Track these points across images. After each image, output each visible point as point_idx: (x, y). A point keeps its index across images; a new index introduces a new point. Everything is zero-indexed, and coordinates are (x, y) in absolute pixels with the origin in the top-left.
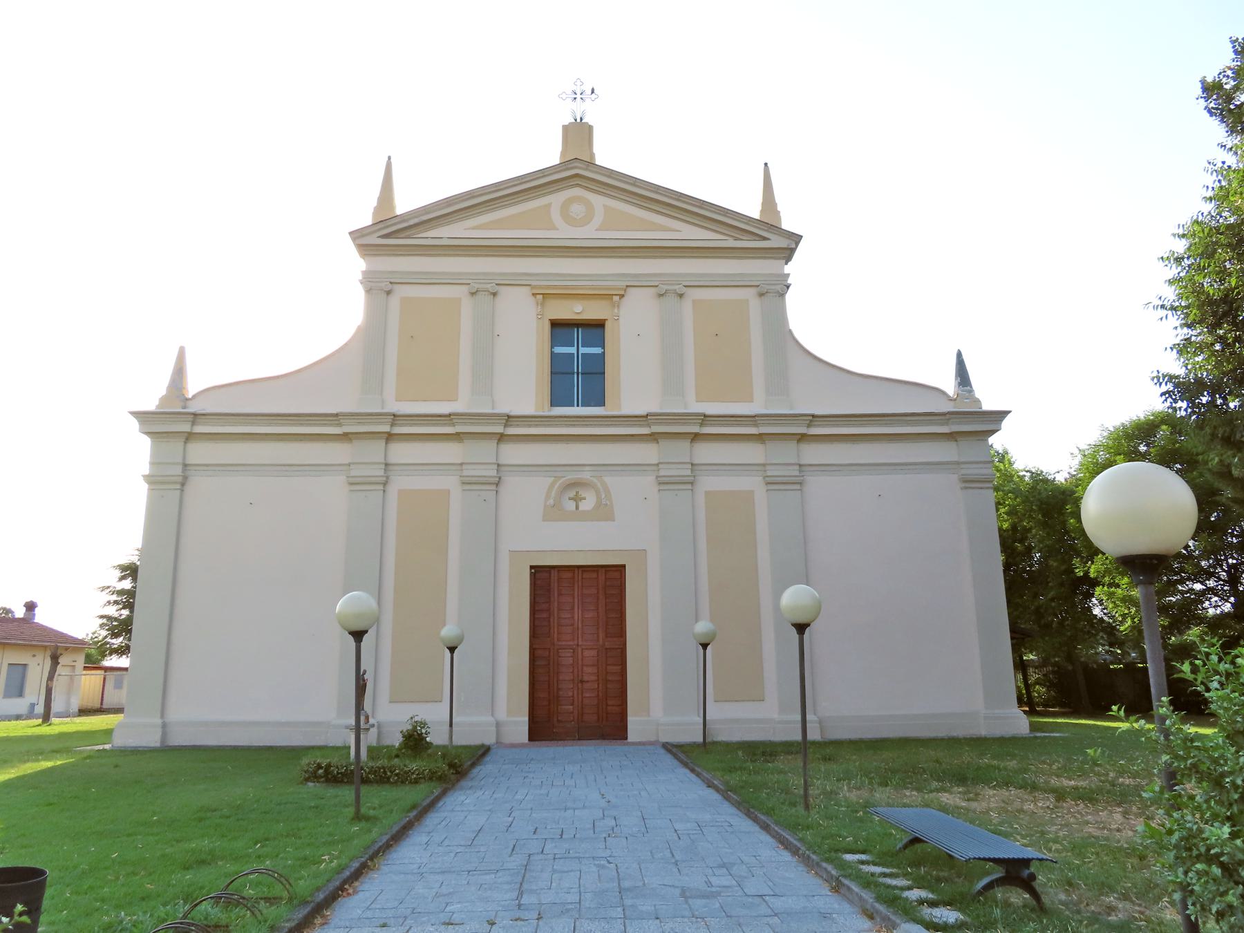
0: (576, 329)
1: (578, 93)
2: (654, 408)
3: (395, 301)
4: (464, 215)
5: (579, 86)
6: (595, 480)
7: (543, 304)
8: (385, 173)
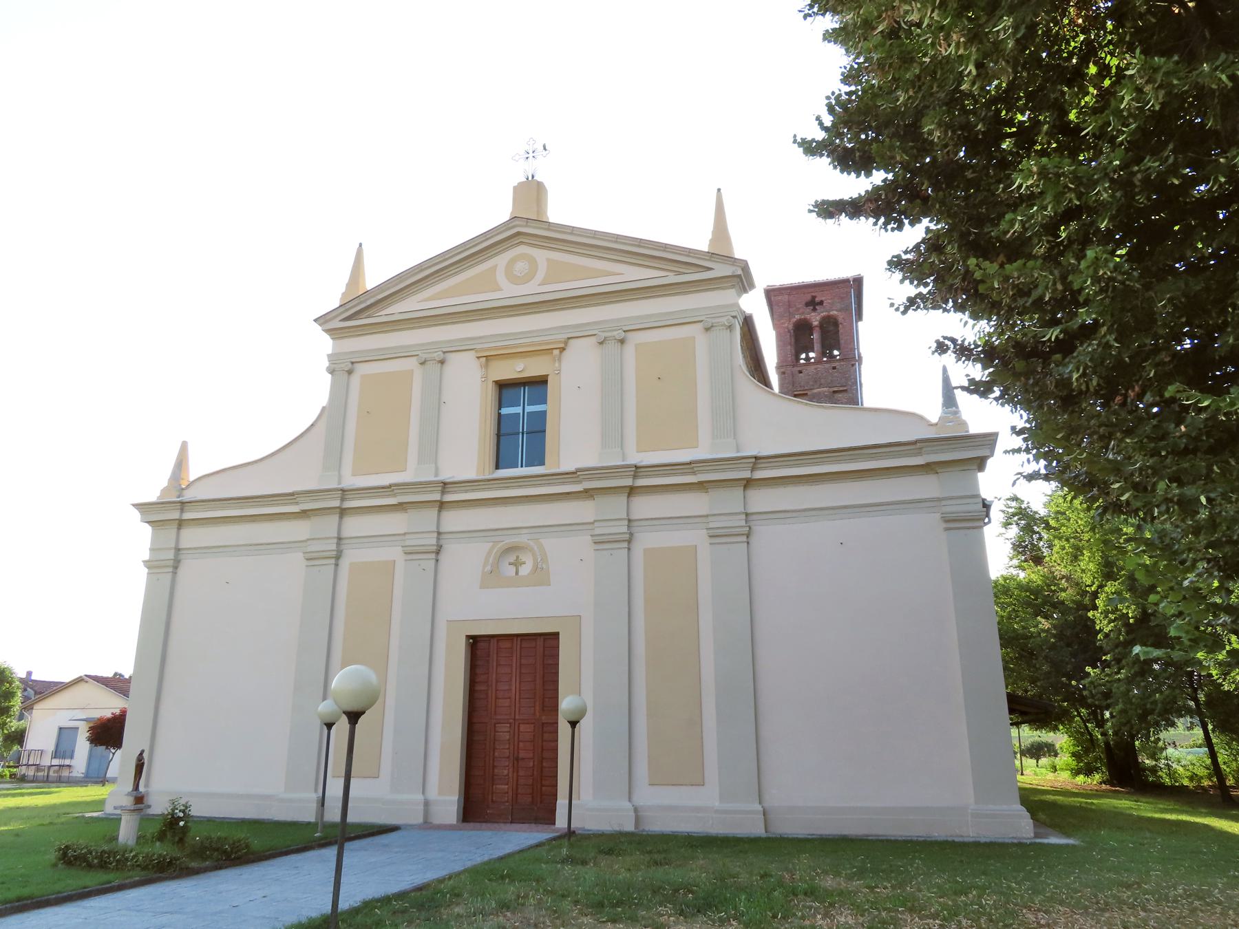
0: (522, 388)
1: (531, 152)
2: (591, 461)
3: (356, 380)
4: (425, 285)
5: (531, 145)
6: (531, 543)
7: (486, 366)
8: (355, 262)
